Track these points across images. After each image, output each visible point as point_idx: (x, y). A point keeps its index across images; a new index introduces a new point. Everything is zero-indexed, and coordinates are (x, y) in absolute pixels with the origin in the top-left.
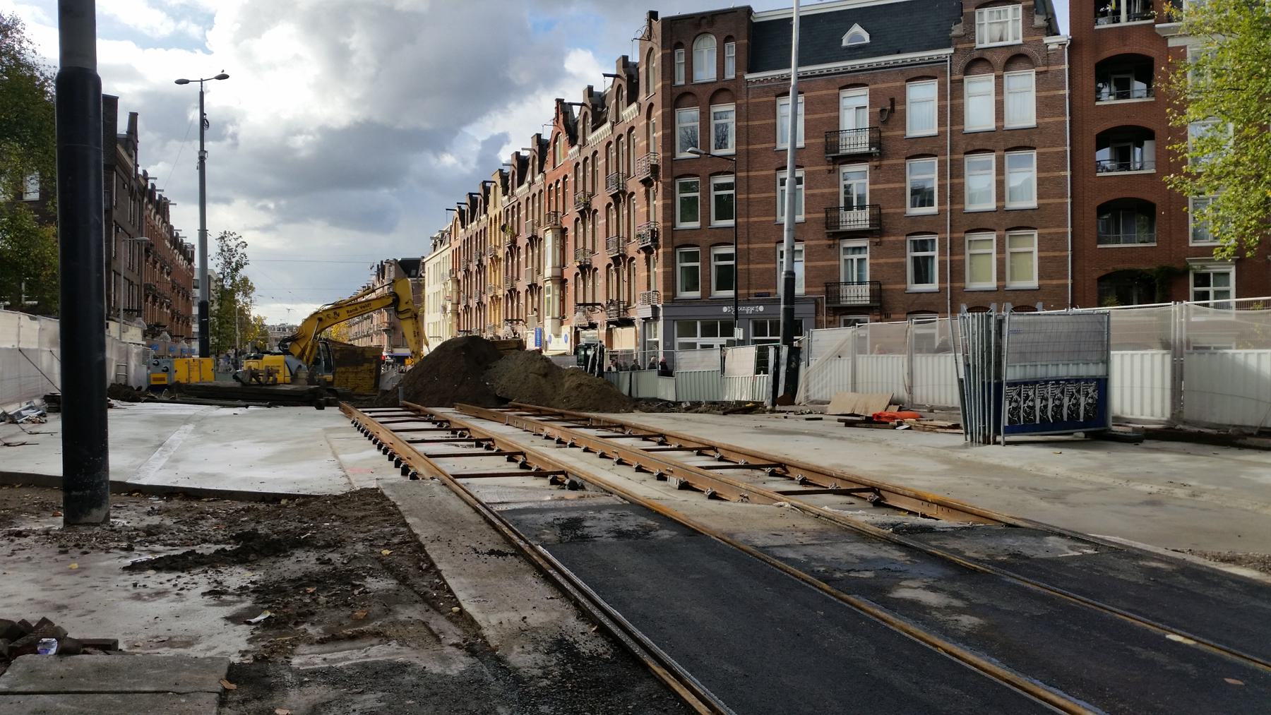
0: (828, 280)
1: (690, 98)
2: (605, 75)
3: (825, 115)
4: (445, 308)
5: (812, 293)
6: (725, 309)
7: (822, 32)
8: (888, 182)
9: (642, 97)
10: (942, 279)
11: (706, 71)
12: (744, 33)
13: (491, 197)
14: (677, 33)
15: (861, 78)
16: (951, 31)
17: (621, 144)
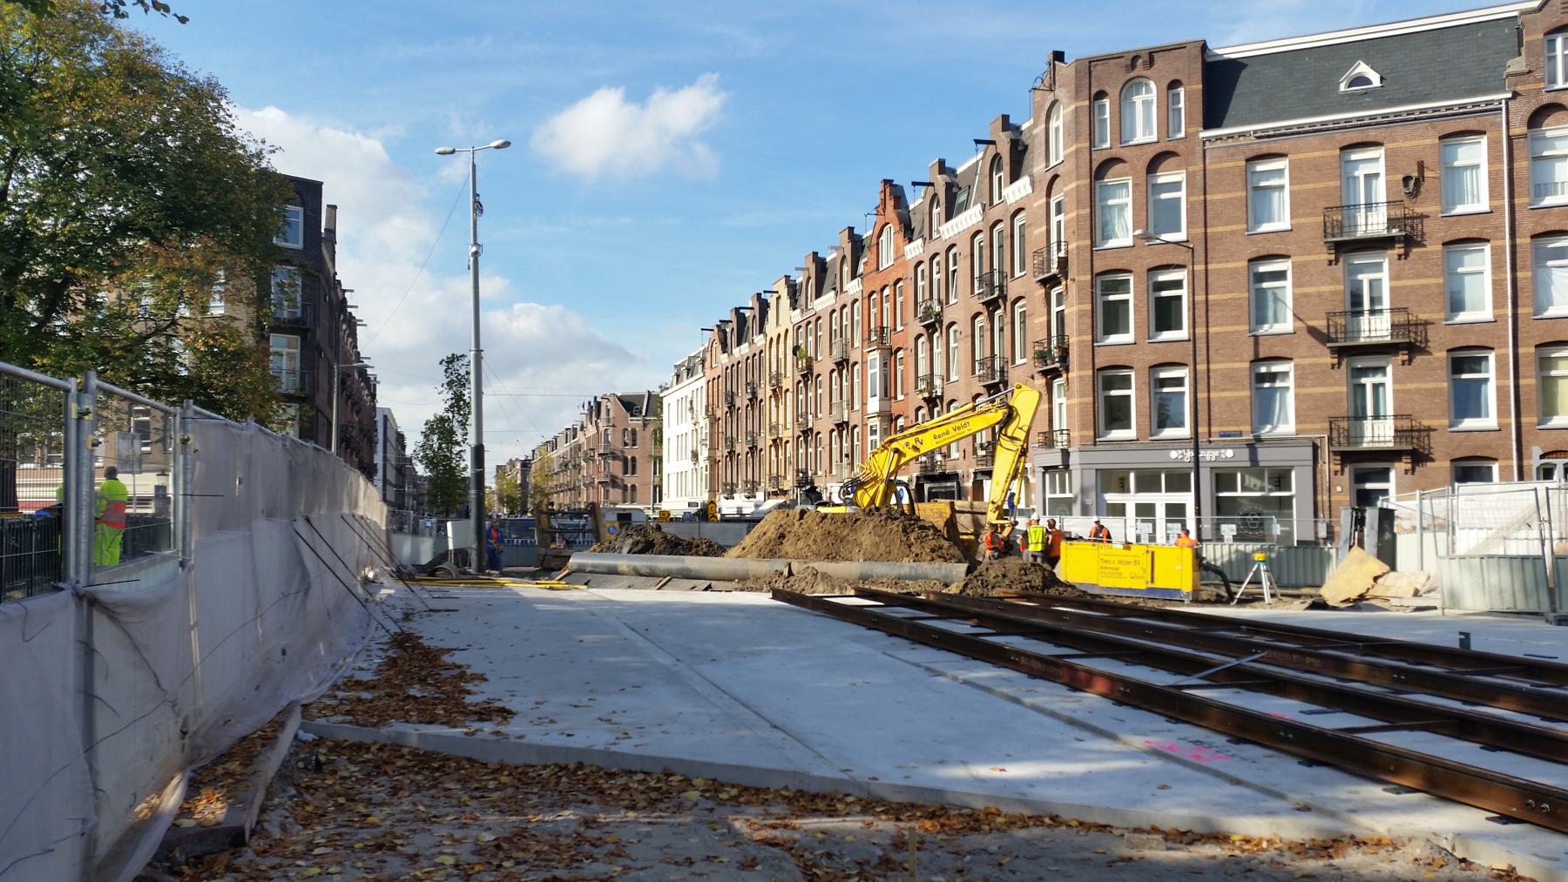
0: (1332, 413)
1: (1119, 167)
2: (978, 142)
3: (1321, 185)
4: (695, 455)
5: (1310, 431)
6: (1174, 454)
7: (1308, 75)
8: (1418, 276)
9: (1039, 168)
10: (1502, 412)
11: (1145, 131)
12: (1198, 75)
13: (772, 313)
14: (1102, 80)
15: (1372, 134)
16: (1505, 67)
17: (1002, 232)
